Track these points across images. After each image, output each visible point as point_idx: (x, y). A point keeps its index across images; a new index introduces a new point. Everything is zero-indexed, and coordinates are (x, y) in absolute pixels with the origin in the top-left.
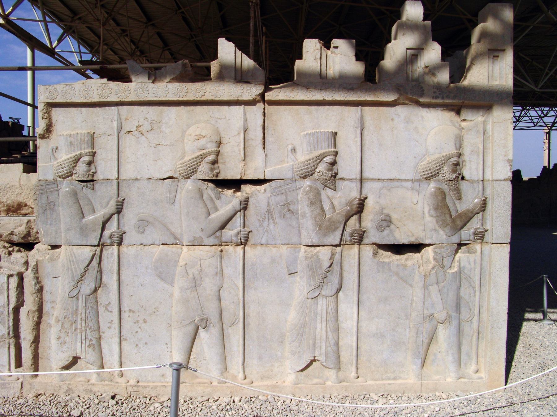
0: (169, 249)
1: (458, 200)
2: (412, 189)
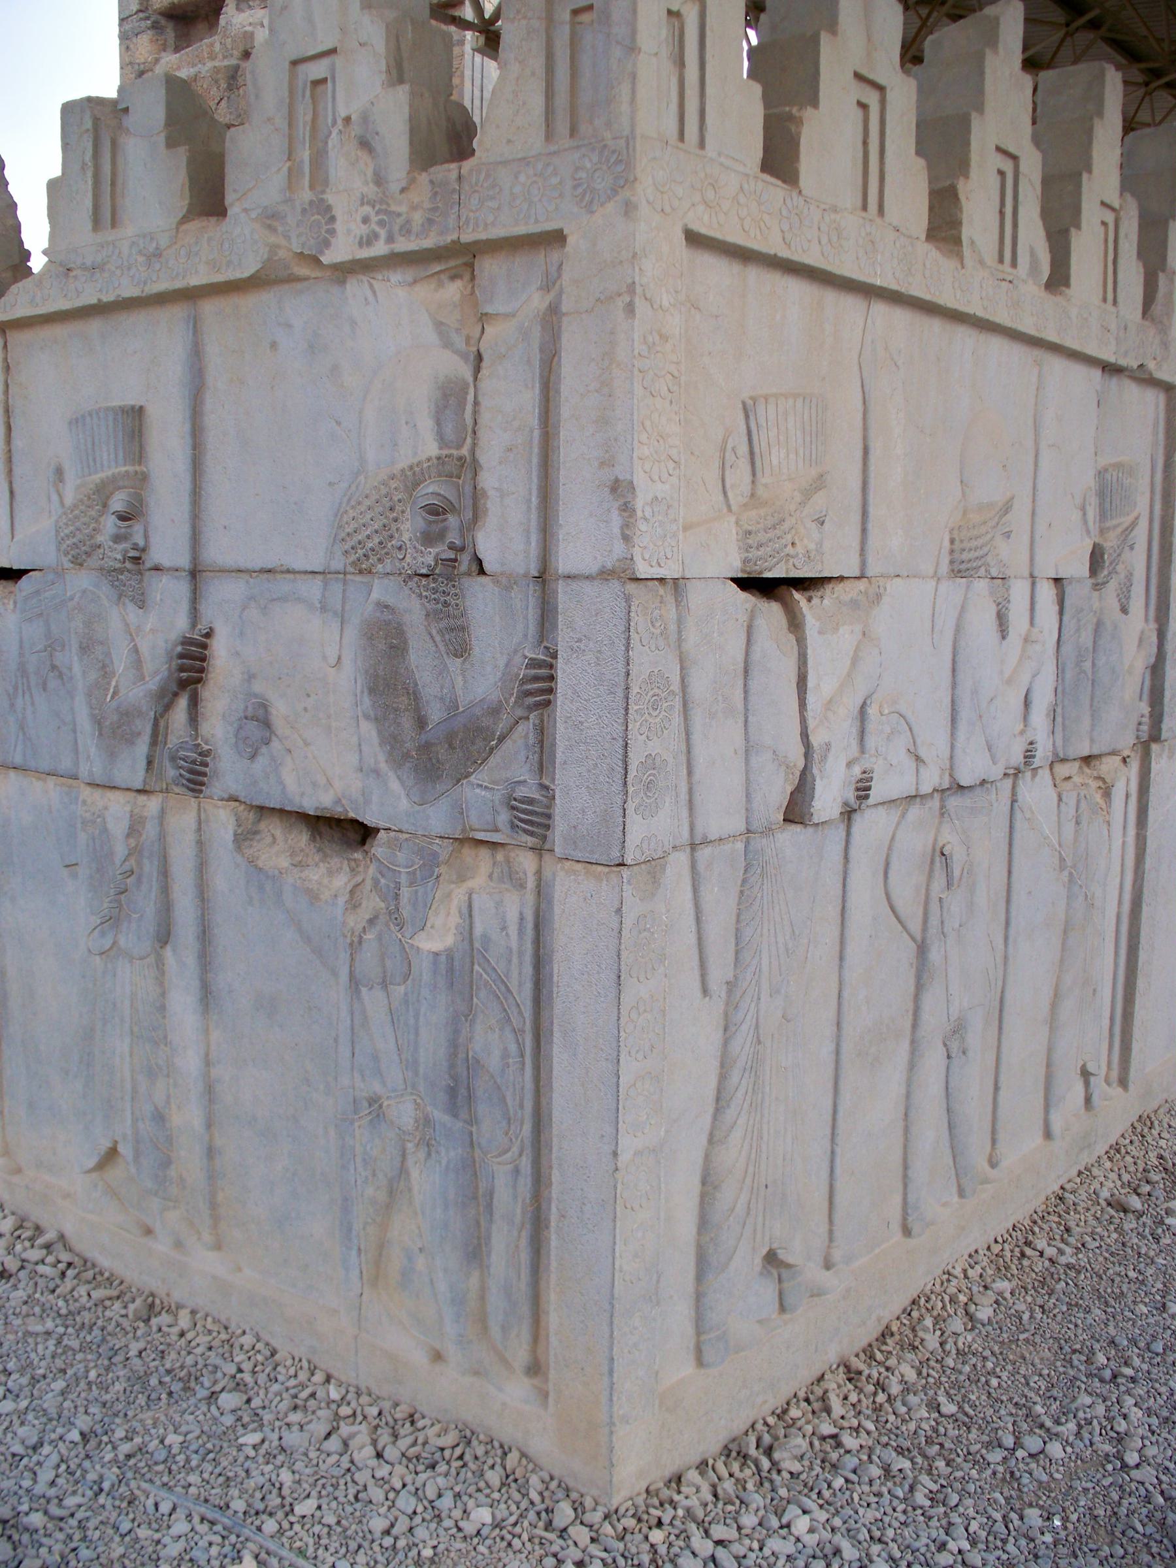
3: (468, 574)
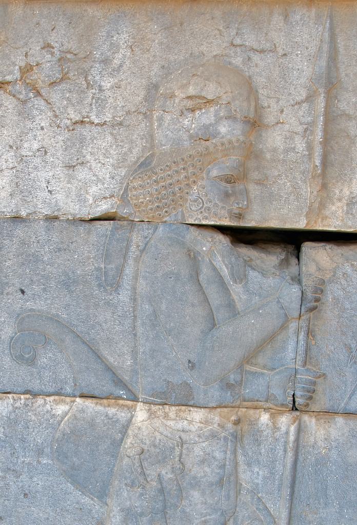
0: (100, 408)
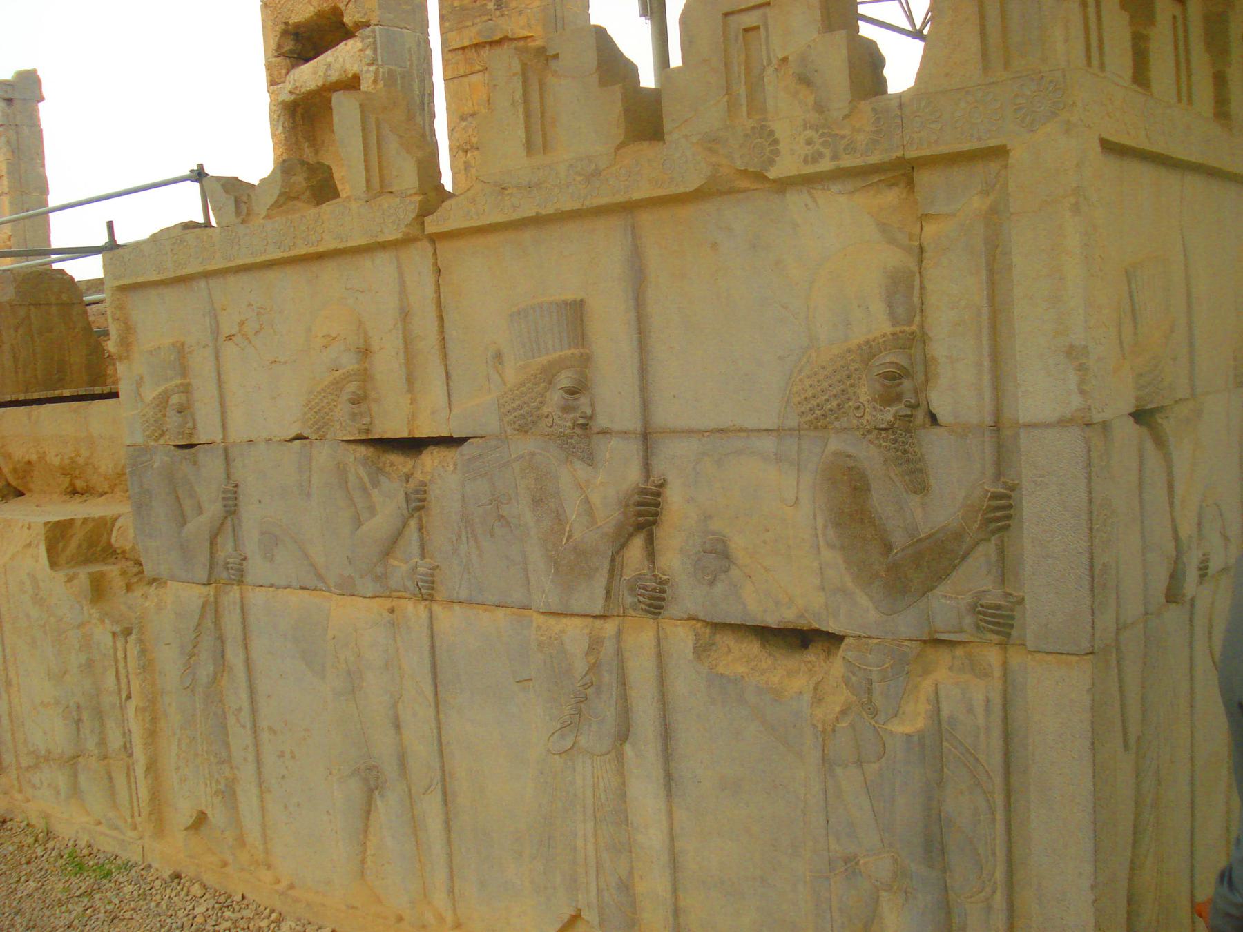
1: (915, 492)
2: (779, 458)
3: (923, 426)
